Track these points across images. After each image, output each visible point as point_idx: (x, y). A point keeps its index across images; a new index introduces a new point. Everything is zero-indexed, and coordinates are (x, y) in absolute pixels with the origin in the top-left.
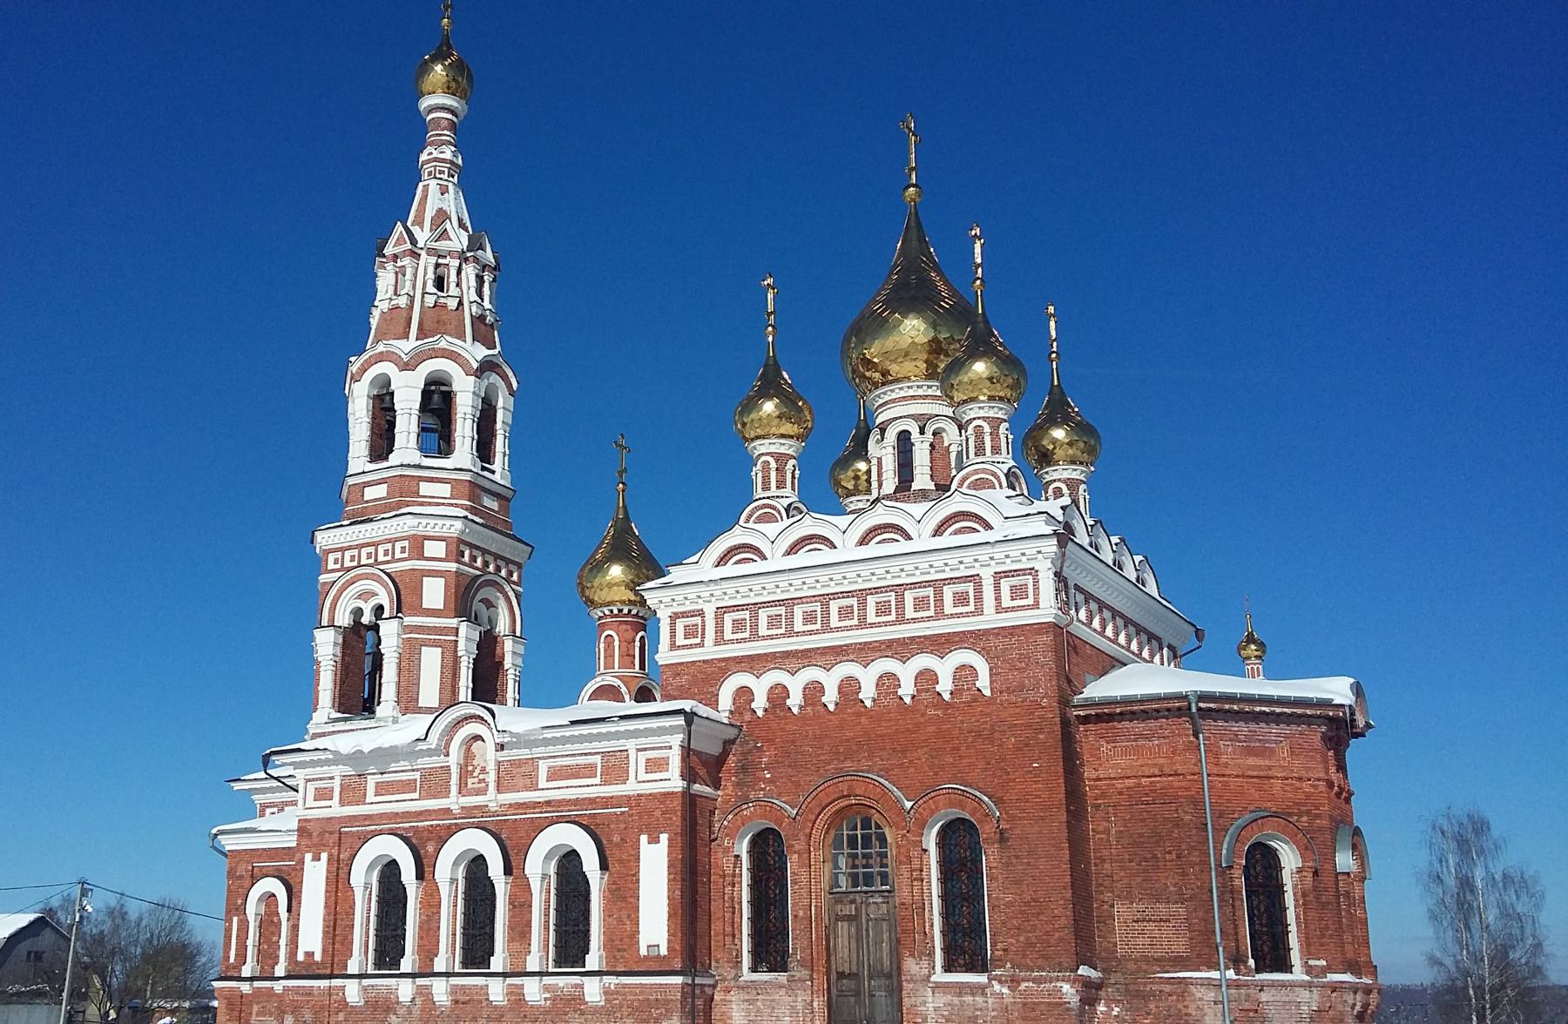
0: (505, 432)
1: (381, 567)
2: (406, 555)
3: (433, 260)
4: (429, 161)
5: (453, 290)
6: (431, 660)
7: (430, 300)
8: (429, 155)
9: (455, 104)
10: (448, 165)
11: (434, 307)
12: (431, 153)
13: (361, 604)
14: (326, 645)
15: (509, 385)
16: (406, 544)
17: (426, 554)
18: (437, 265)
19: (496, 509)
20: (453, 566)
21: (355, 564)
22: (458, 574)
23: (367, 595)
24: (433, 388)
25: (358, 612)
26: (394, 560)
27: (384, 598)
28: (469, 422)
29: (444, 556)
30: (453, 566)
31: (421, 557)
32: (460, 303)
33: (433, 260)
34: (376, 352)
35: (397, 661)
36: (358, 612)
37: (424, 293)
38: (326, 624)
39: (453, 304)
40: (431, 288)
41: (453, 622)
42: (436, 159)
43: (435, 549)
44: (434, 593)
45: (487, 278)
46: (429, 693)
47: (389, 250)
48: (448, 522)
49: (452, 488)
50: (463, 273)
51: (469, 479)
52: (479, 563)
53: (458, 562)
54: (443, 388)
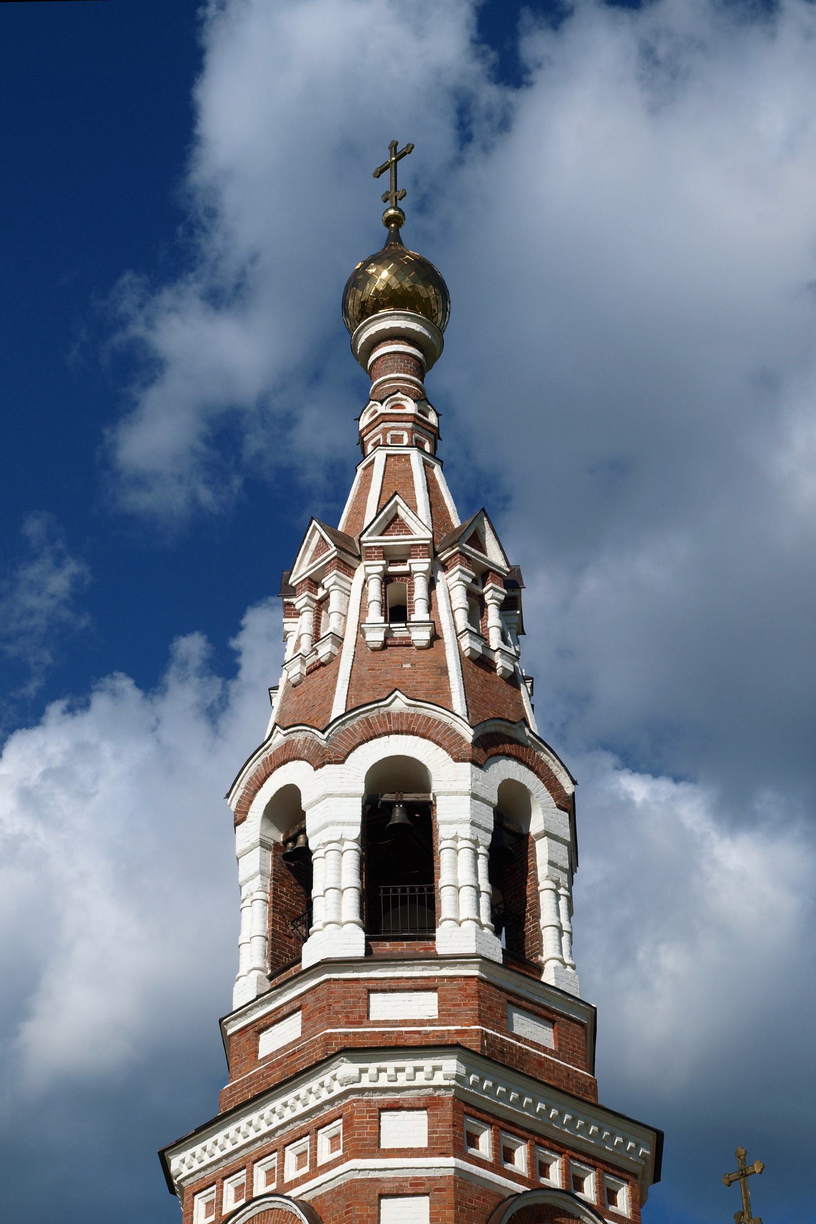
0: (557, 883)
1: (293, 1193)
2: (339, 1153)
4: (371, 426)
7: (376, 637)
8: (372, 415)
9: (415, 326)
10: (410, 425)
11: (385, 646)
12: (376, 412)
15: (552, 785)
17: (385, 1144)
18: (387, 579)
19: (552, 1045)
22: (461, 1178)
24: (388, 797)
26: (316, 1170)
28: (465, 857)
29: (424, 1144)
31: (373, 1148)
32: (436, 637)
33: (376, 567)
34: (270, 751)
39: (421, 636)
40: (375, 615)
42: (384, 418)
45: (492, 594)
47: (302, 569)
49: (441, 1000)
50: (440, 588)
51: (476, 973)
52: (520, 1161)
53: (460, 1152)
54: (409, 797)
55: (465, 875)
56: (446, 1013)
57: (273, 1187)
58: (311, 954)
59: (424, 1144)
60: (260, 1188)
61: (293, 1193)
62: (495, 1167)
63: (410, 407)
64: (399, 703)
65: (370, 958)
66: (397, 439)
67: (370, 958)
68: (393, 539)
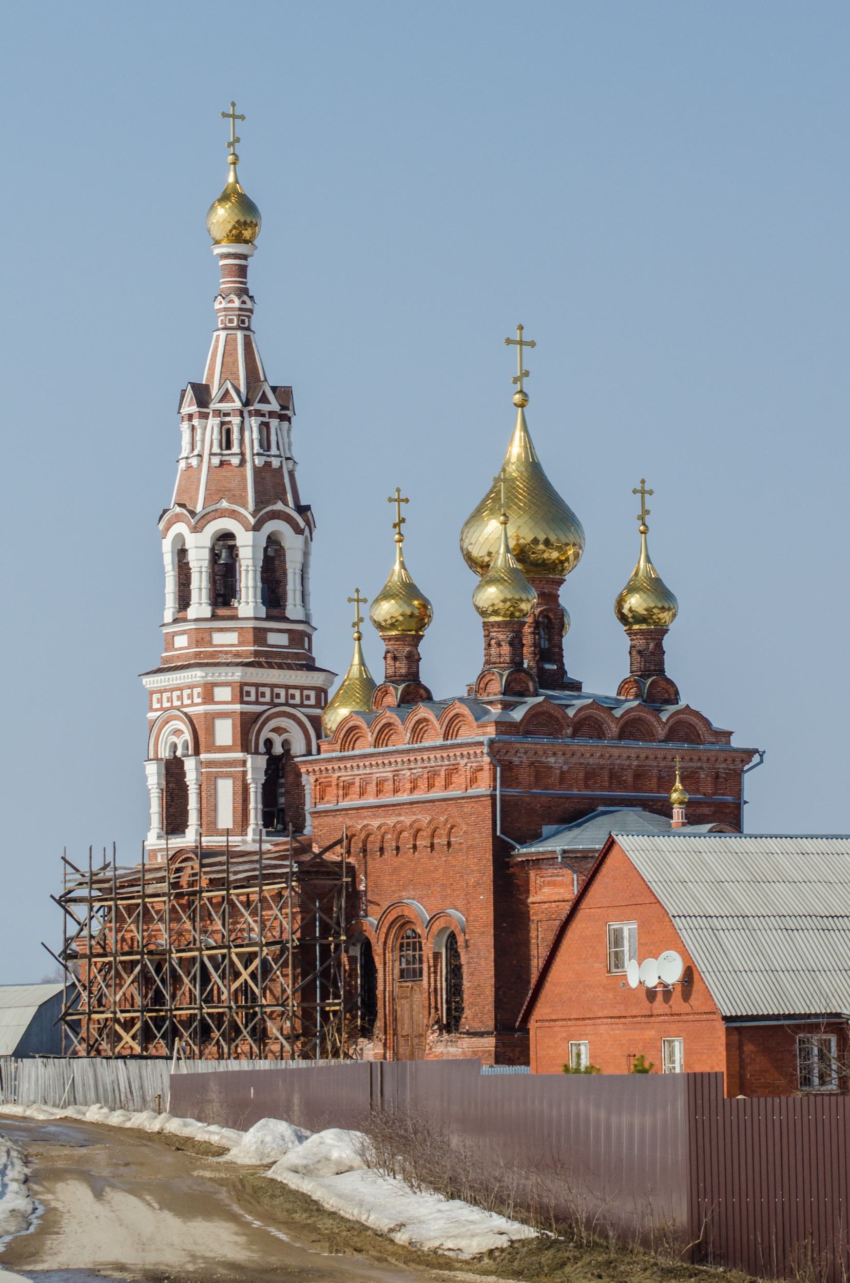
3: (217, 420)
5: (235, 449)
6: (226, 789)
7: (216, 461)
13: (174, 739)
14: (153, 775)
16: (199, 690)
17: (216, 699)
20: (238, 707)
21: (169, 705)
23: (178, 732)
25: (174, 746)
26: (193, 704)
27: (187, 736)
29: (230, 700)
30: (238, 707)
33: (217, 420)
35: (198, 791)
36: (174, 746)
37: (211, 454)
38: (152, 757)
39: (235, 461)
41: (240, 755)
43: (223, 694)
44: (225, 732)
46: (226, 818)
48: (230, 670)
53: (242, 702)
55: (251, 583)
56: (241, 643)
57: (179, 703)
58: (192, 613)
59: (230, 700)
60: (177, 703)
61: (185, 710)
62: (257, 702)
63: (237, 304)
64: (225, 504)
65: (214, 617)
66: (231, 321)
67: (214, 617)
68: (224, 406)
